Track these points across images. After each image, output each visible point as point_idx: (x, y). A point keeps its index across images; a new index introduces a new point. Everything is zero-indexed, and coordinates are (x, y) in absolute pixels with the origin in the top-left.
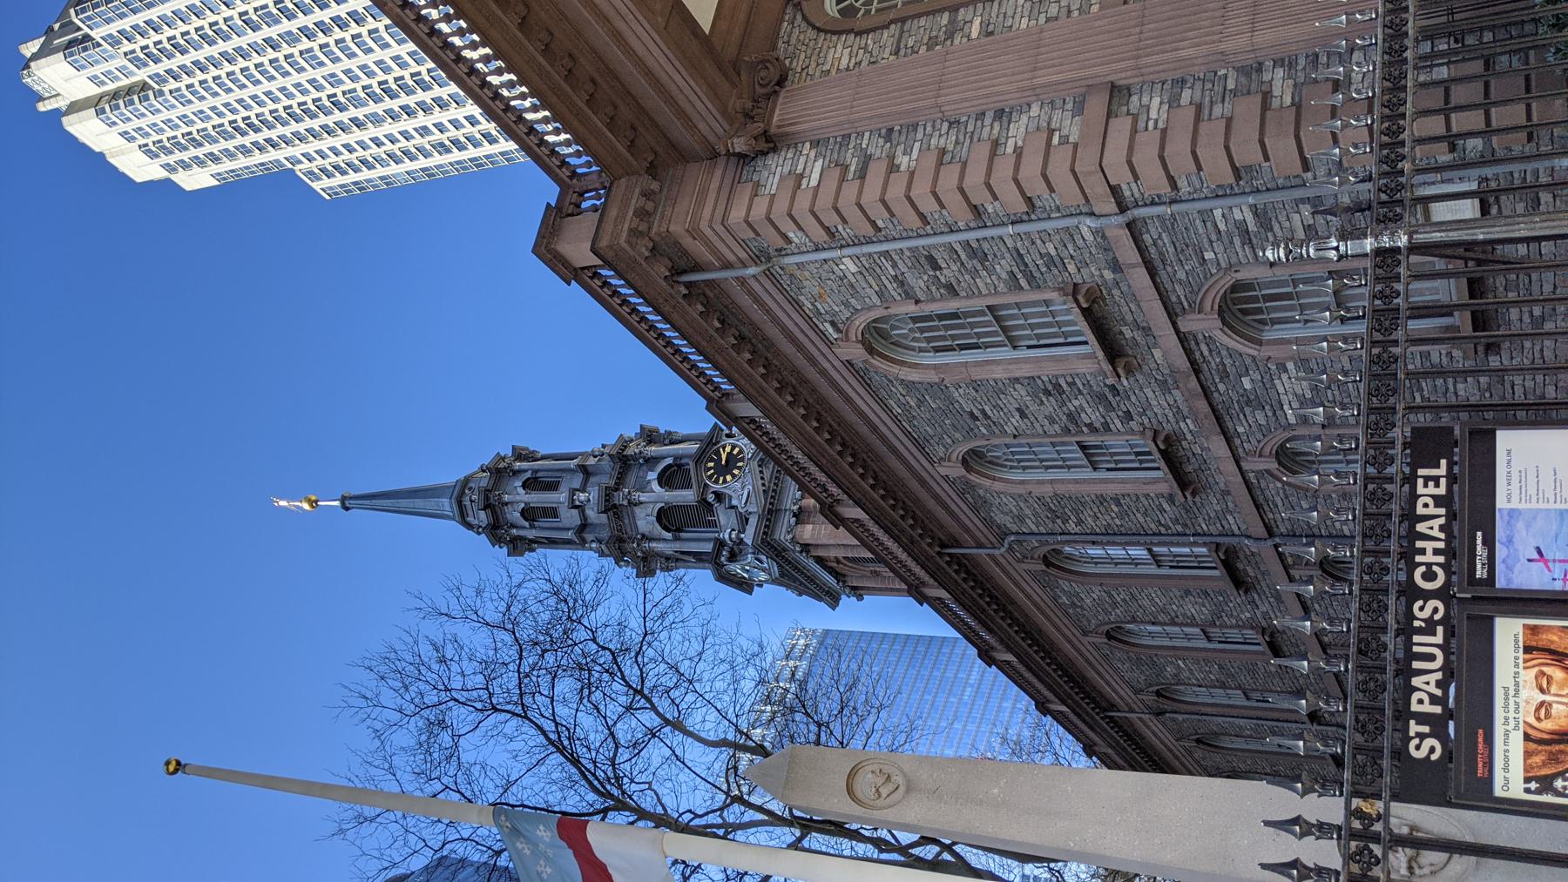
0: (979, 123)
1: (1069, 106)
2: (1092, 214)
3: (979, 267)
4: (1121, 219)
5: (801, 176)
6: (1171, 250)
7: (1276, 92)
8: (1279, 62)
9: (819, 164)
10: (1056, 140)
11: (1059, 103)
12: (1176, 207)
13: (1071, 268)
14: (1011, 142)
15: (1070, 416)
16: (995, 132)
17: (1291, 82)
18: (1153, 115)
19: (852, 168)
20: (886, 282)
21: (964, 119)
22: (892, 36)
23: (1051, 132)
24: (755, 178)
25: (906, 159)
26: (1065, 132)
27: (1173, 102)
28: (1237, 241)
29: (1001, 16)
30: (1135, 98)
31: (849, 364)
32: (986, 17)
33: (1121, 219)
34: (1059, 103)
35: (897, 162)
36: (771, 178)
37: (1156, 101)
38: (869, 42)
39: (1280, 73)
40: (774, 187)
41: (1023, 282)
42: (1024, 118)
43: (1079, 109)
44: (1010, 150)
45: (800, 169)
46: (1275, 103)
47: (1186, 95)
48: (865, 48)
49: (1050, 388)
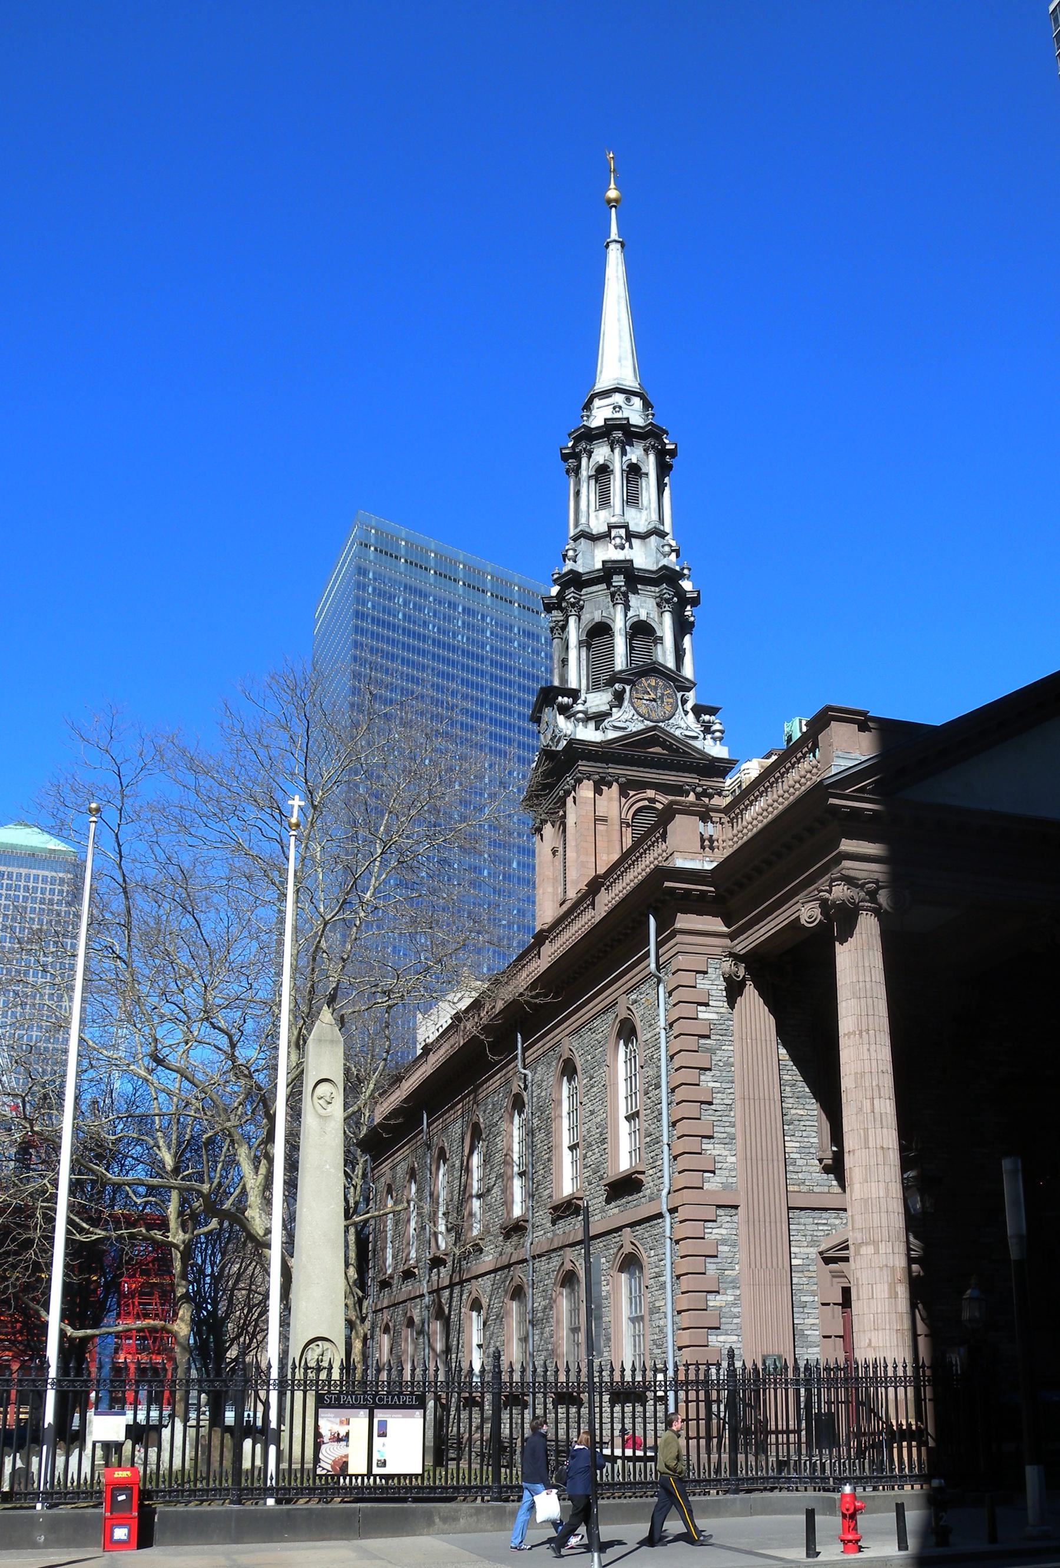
0: (728, 1124)
1: (730, 1180)
2: (669, 1193)
3: (654, 1115)
4: (664, 1209)
5: (707, 1005)
6: (655, 1232)
7: (718, 1297)
8: (738, 1298)
9: (714, 1016)
10: (706, 1175)
11: (733, 1173)
12: (668, 1240)
13: (651, 1172)
14: (710, 1146)
15: (590, 1145)
16: (720, 1135)
17: (724, 1305)
18: (715, 1231)
19: (708, 1041)
20: (651, 1050)
21: (732, 1114)
23: (713, 1172)
24: (710, 970)
25: (709, 1079)
26: (712, 1180)
27: (724, 1242)
28: (657, 1270)
29: (804, 1128)
30: (728, 1219)
31: (614, 1003)
32: (804, 1118)
33: (664, 1209)
34: (733, 1173)
35: (707, 1073)
36: (710, 982)
37: (724, 1231)
39: (731, 1298)
40: (702, 986)
41: (648, 1139)
42: (727, 1153)
43: (726, 1187)
44: (704, 1147)
45: (711, 1003)
46: (710, 1297)
47: (726, 1248)
49: (604, 1137)
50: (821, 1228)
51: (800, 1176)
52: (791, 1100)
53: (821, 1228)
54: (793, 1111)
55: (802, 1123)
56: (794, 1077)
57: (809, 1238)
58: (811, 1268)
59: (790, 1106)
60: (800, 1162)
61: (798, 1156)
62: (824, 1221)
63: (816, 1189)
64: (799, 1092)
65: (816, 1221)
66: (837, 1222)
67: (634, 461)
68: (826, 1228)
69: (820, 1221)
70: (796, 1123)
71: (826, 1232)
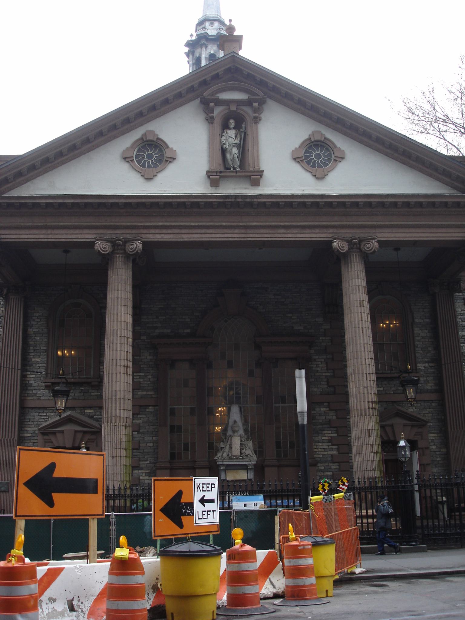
22: (42, 330)
38: (42, 322)
48: (40, 321)
50: (42, 417)
51: (34, 391)
52: (32, 354)
53: (42, 417)
54: (33, 360)
55: (38, 365)
56: (35, 343)
57: (35, 423)
58: (35, 438)
59: (32, 357)
60: (35, 385)
61: (34, 382)
62: (45, 414)
63: (42, 398)
64: (38, 349)
65: (40, 414)
66: (52, 414)
67: (212, 52)
68: (45, 417)
69: (42, 414)
70: (34, 365)
71: (45, 420)
